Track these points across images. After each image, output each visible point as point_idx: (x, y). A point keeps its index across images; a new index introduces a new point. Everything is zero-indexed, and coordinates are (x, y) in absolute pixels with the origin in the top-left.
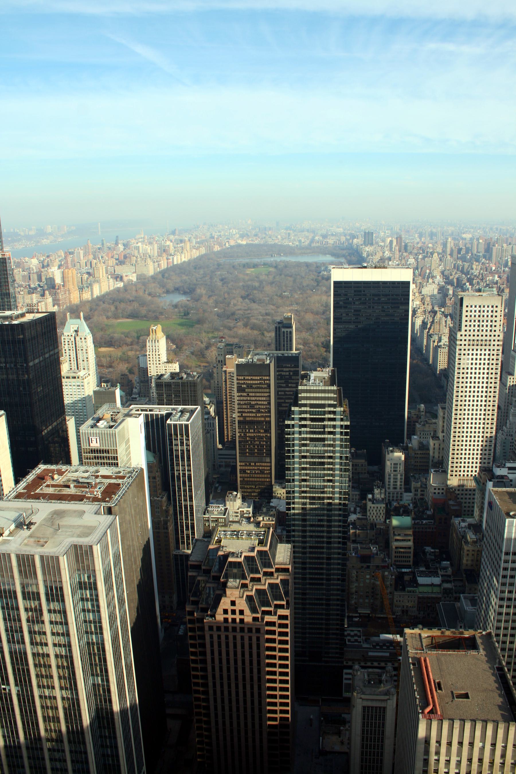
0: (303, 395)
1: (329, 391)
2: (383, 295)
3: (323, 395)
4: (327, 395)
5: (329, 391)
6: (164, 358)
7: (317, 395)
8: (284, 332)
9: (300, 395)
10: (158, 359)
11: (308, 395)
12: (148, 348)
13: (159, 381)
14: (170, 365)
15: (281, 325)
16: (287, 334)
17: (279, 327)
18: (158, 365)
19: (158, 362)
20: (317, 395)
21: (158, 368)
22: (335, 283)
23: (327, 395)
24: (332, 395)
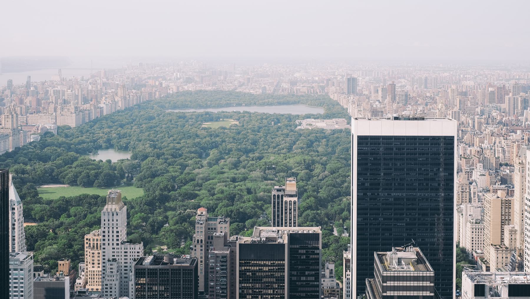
0: (389, 284)
1: (423, 279)
2: (420, 154)
3: (416, 284)
4: (421, 284)
5: (423, 279)
6: (123, 236)
7: (408, 284)
8: (286, 202)
9: (385, 284)
10: (115, 238)
11: (396, 284)
12: (102, 222)
13: (140, 267)
14: (132, 246)
15: (280, 193)
16: (290, 204)
17: (278, 196)
18: (115, 246)
19: (115, 242)
20: (408, 284)
21: (115, 250)
22: (360, 138)
23: (421, 284)
24: (428, 284)
